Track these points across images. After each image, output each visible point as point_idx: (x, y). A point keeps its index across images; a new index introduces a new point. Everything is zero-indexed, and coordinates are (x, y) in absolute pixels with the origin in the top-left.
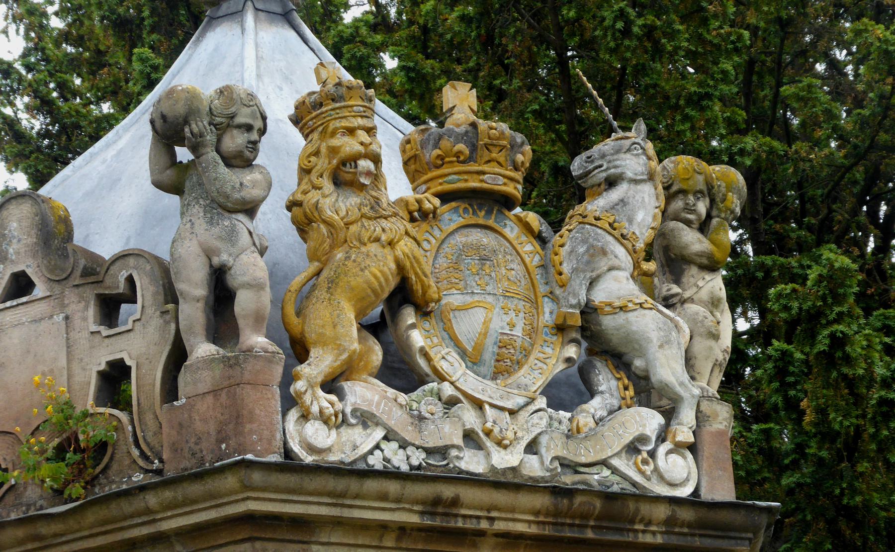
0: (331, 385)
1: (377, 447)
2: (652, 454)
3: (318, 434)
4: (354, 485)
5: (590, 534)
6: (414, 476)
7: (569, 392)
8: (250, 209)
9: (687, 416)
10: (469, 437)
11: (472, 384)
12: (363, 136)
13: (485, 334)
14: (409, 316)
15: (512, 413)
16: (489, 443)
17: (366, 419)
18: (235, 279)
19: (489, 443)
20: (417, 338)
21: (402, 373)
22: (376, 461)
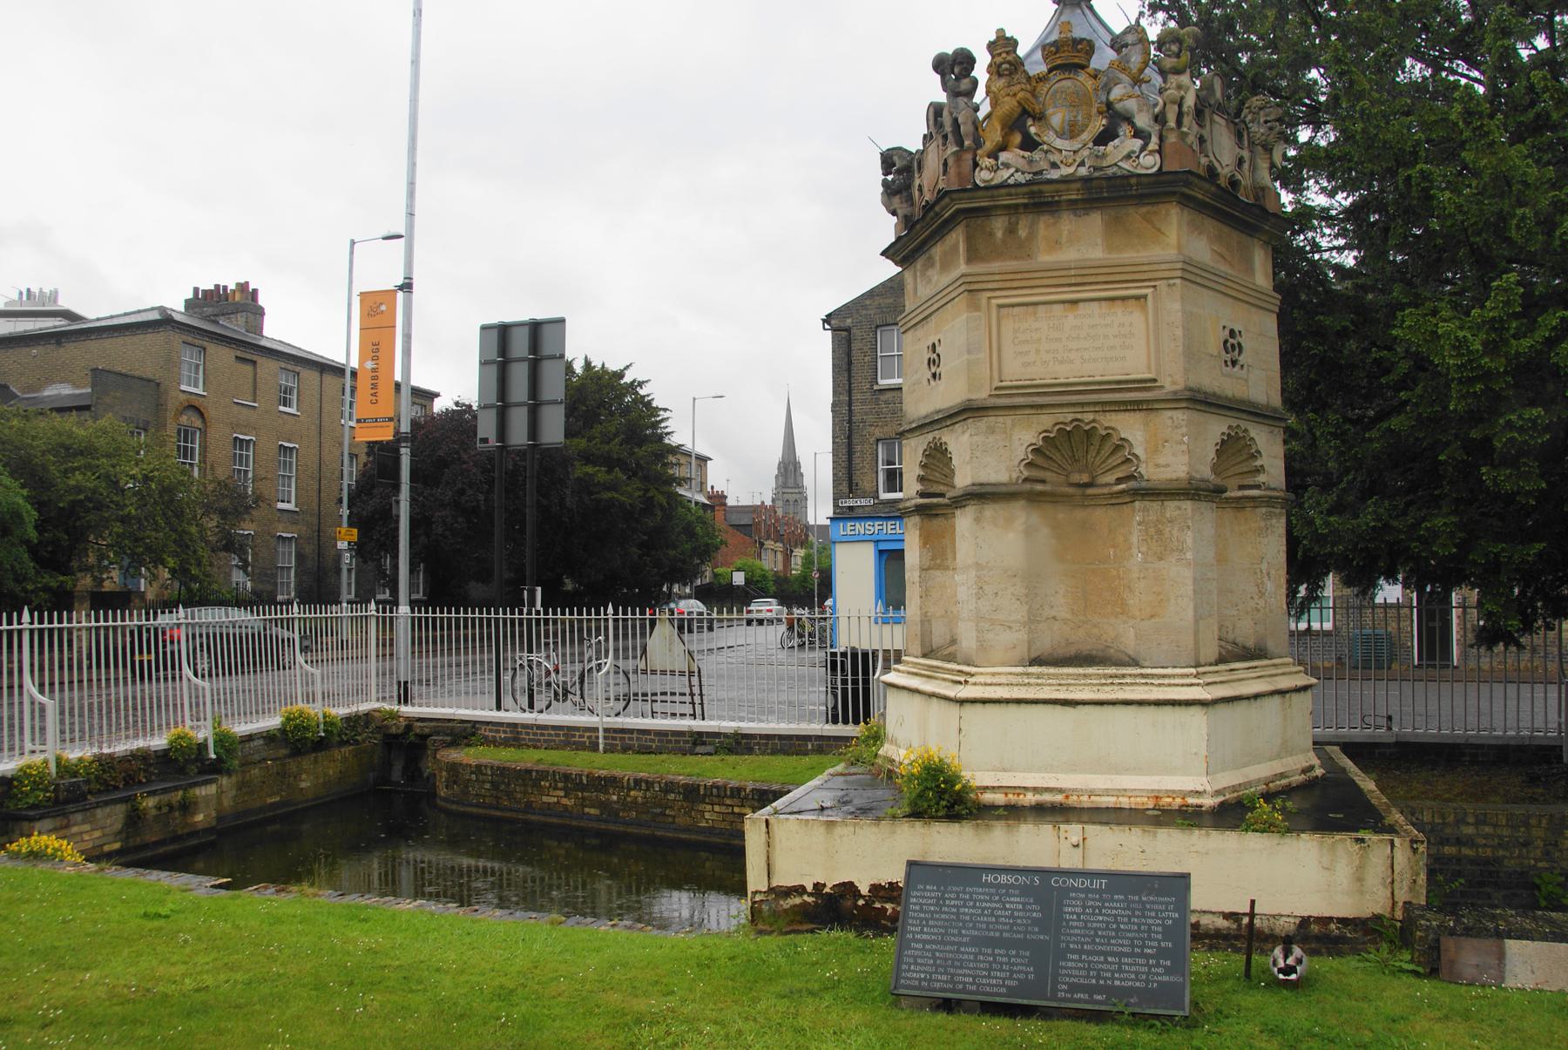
4: (996, 192)
6: (1029, 183)
7: (1104, 138)
8: (970, 93)
10: (1054, 165)
11: (1059, 143)
14: (1030, 122)
17: (1007, 166)
20: (1033, 130)
21: (1029, 144)
22: (1011, 181)
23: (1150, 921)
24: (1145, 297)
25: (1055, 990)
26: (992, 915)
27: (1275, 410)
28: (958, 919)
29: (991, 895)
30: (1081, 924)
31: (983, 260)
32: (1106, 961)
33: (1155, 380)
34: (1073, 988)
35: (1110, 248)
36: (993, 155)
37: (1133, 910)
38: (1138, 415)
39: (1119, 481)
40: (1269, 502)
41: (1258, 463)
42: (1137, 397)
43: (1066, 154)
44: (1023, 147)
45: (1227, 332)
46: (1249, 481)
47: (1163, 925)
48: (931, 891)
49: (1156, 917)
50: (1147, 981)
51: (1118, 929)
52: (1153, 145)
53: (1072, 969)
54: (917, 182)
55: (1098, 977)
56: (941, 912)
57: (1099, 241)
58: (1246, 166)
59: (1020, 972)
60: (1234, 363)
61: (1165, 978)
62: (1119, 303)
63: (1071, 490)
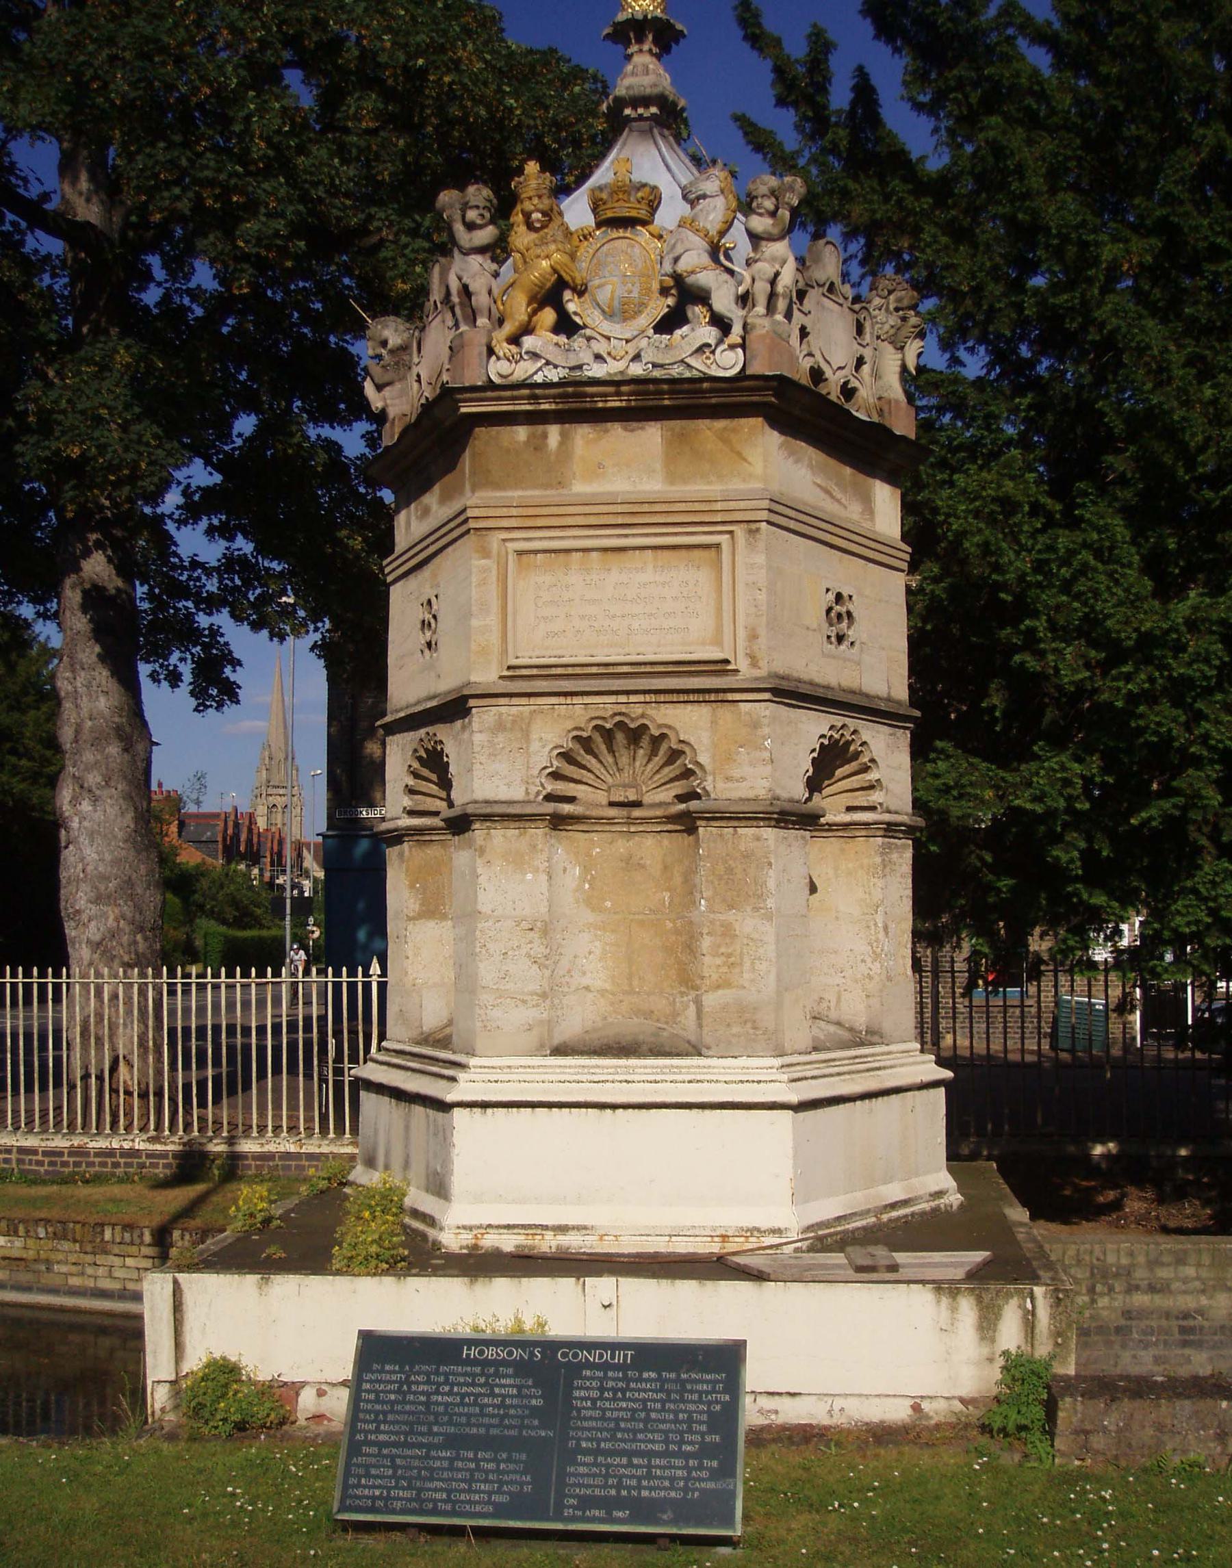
0: (515, 340)
1: (540, 369)
2: (713, 352)
3: (503, 367)
5: (667, 402)
6: (561, 384)
7: (667, 325)
9: (737, 329)
10: (598, 357)
11: (606, 327)
12: (536, 201)
13: (612, 299)
15: (627, 341)
16: (609, 359)
17: (535, 356)
18: (471, 289)
19: (609, 359)
20: (571, 307)
21: (566, 326)
22: (539, 378)
23: (692, 1407)
24: (717, 546)
25: (560, 1506)
26: (475, 1404)
27: (899, 703)
28: (428, 1411)
29: (474, 1375)
30: (597, 1413)
31: (498, 486)
32: (630, 1465)
33: (727, 662)
34: (586, 1503)
35: (671, 477)
36: (515, 340)
37: (668, 1392)
38: (705, 710)
39: (681, 798)
40: (890, 829)
41: (873, 776)
42: (705, 682)
43: (617, 347)
44: (556, 330)
45: (831, 596)
46: (861, 799)
47: (709, 1412)
48: (392, 1372)
49: (700, 1401)
50: (686, 1489)
51: (647, 1420)
52: (735, 336)
53: (583, 1475)
54: (415, 370)
55: (619, 1486)
56: (404, 1402)
57: (658, 466)
58: (866, 369)
59: (511, 1482)
60: (840, 639)
61: (711, 1485)
62: (683, 553)
63: (613, 812)
